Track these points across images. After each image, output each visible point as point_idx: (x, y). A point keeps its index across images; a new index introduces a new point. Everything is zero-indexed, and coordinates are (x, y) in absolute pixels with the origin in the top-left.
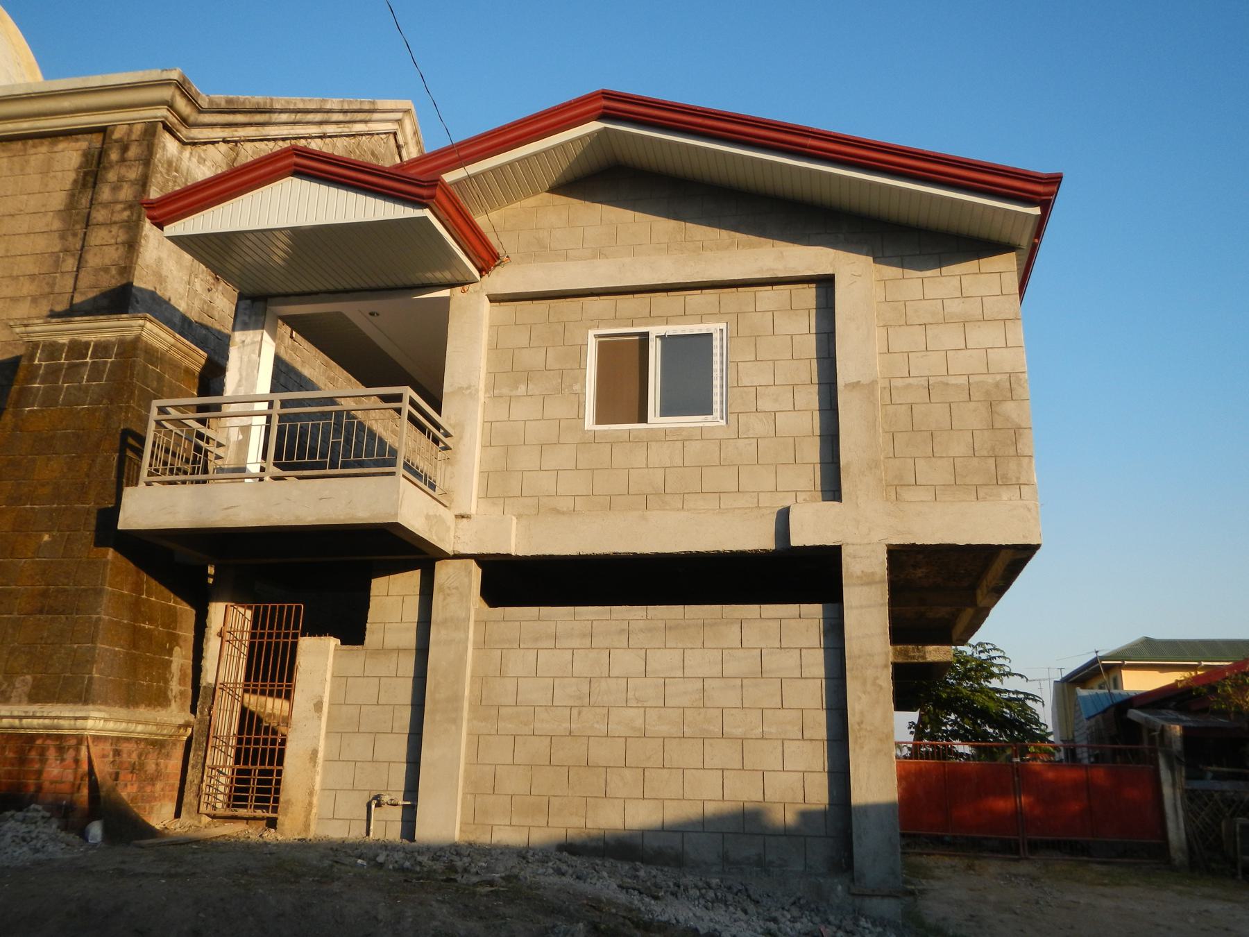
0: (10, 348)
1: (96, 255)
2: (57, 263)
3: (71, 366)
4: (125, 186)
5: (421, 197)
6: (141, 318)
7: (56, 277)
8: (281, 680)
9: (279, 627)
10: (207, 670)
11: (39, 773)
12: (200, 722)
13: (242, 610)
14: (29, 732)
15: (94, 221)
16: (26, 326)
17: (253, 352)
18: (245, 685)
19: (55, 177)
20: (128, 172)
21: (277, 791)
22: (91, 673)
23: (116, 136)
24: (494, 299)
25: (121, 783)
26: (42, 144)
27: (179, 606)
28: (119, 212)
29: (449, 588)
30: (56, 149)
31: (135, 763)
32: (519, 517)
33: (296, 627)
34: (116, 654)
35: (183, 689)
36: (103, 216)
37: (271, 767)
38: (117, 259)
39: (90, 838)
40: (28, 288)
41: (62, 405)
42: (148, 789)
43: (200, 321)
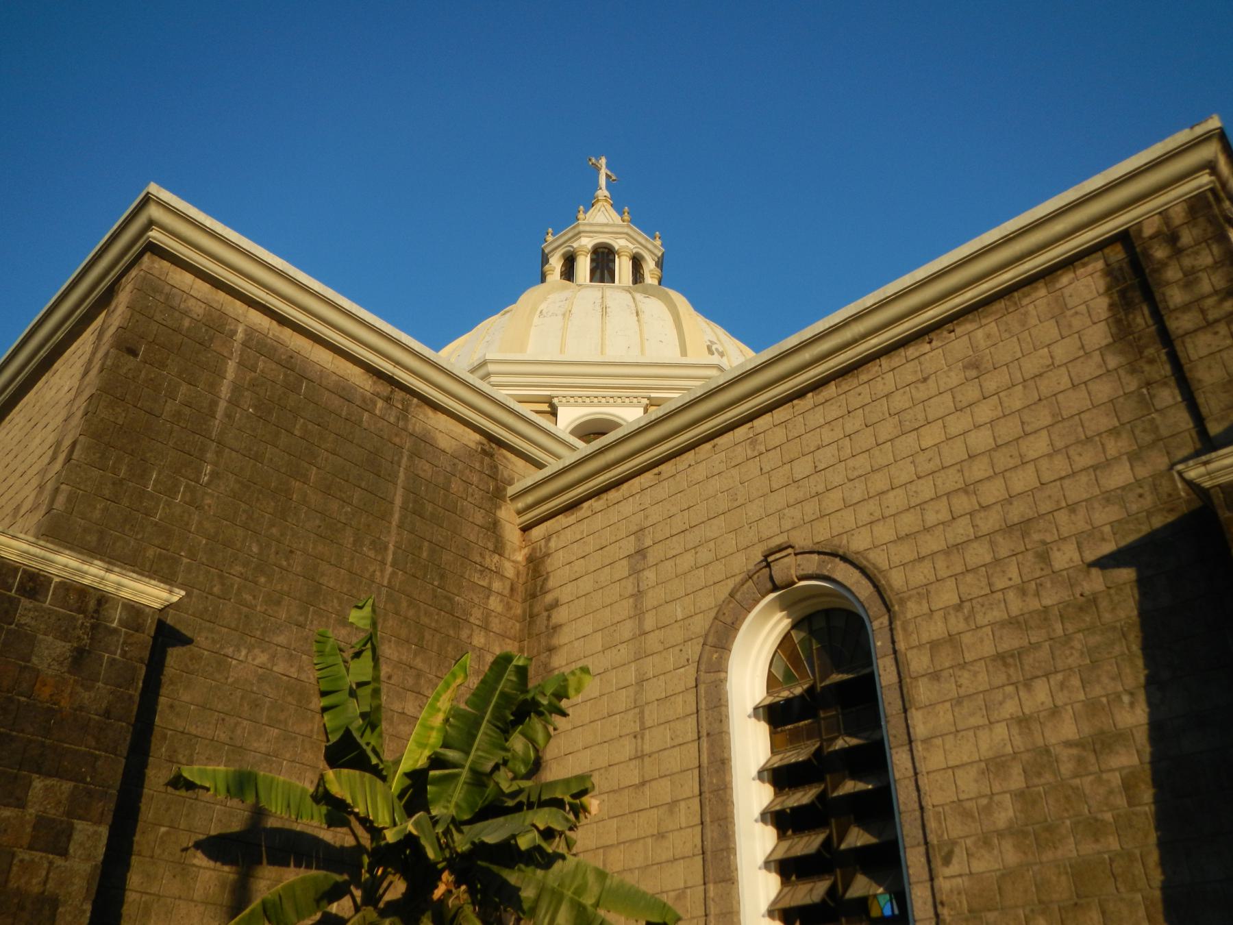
0: (1132, 527)
1: (1210, 368)
2: (1146, 403)
4: (1204, 275)
7: (1153, 418)
15: (1181, 332)
16: (1205, 463)
19: (1076, 313)
23: (1148, 231)
26: (1036, 289)
28: (1213, 307)
30: (1058, 286)
40: (1113, 447)
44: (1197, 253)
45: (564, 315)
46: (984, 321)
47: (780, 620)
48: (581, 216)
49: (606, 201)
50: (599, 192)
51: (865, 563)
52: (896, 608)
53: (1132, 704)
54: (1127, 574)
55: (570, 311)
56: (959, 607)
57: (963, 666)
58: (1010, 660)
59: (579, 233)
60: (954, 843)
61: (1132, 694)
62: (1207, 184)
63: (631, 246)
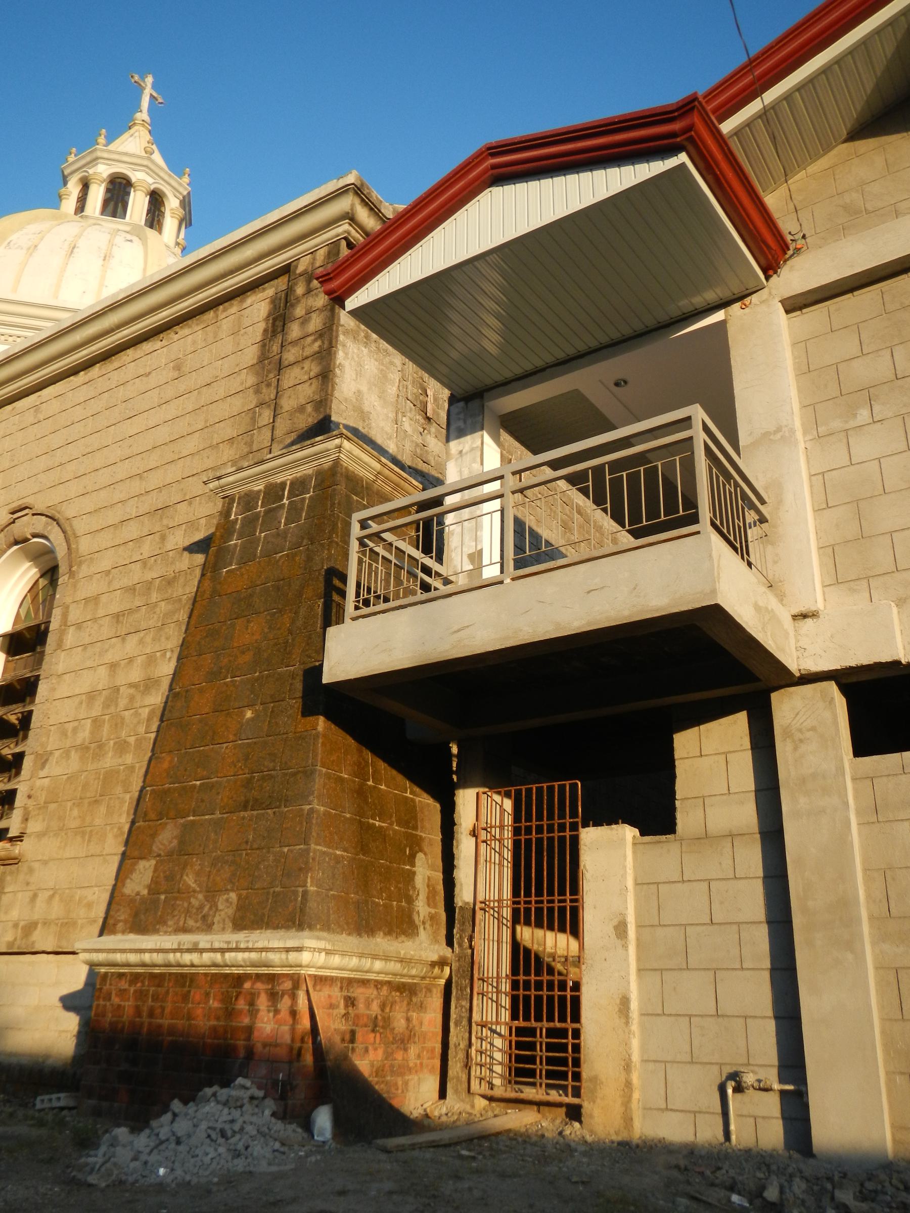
1: (290, 397)
3: (267, 512)
5: (673, 135)
6: (337, 437)
8: (562, 892)
9: (551, 817)
10: (461, 885)
11: (250, 1030)
12: (460, 957)
13: (497, 798)
14: (235, 971)
16: (219, 478)
17: (474, 461)
18: (514, 903)
20: (314, 301)
21: (577, 1063)
22: (305, 886)
23: (301, 268)
24: (794, 305)
25: (359, 1045)
26: (232, 305)
27: (417, 799)
29: (800, 731)
31: (376, 1017)
32: (900, 602)
33: (574, 814)
34: (338, 860)
35: (433, 911)
36: (294, 354)
37: (563, 1025)
38: (311, 395)
39: (316, 1132)
41: (260, 558)
42: (399, 1056)
43: (414, 466)
44: (317, 295)
45: (29, 249)
46: (196, 328)
47: (28, 569)
48: (102, 140)
49: (143, 126)
50: (138, 115)
51: (68, 529)
52: (73, 569)
53: (170, 658)
54: (200, 558)
55: (36, 246)
56: (108, 573)
57: (94, 620)
58: (121, 618)
59: (97, 158)
60: (51, 753)
61: (172, 651)
62: (342, 234)
63: (150, 180)
